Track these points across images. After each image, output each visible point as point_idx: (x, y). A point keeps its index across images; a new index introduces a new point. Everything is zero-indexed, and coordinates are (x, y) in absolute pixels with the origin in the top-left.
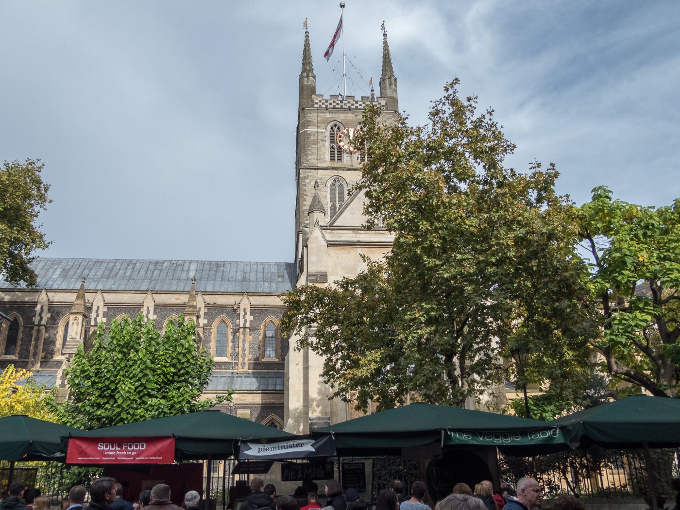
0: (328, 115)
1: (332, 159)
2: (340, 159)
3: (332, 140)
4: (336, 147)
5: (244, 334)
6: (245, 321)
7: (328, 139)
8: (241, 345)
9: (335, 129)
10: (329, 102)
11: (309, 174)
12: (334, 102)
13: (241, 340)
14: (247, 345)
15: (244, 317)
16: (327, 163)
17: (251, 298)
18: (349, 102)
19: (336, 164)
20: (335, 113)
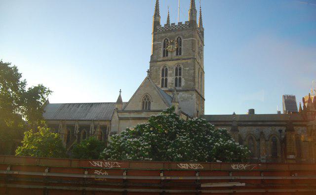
0: (163, 35)
1: (164, 56)
2: (167, 55)
3: (164, 47)
9: (166, 41)
16: (162, 59)
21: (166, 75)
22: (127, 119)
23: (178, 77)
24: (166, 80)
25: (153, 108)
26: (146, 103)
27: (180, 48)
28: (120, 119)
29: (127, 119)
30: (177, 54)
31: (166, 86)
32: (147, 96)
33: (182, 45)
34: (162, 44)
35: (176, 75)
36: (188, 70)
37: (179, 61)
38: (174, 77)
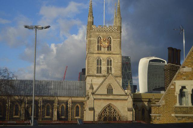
1: (98, 50)
2: (101, 50)
7: (97, 42)
9: (99, 38)
16: (97, 52)
20: (100, 32)
21: (101, 65)
22: (100, 99)
24: (101, 68)
25: (114, 93)
28: (94, 99)
29: (100, 99)
30: (108, 50)
31: (101, 72)
32: (110, 85)
35: (108, 65)
36: (117, 63)
37: (110, 55)
38: (106, 66)
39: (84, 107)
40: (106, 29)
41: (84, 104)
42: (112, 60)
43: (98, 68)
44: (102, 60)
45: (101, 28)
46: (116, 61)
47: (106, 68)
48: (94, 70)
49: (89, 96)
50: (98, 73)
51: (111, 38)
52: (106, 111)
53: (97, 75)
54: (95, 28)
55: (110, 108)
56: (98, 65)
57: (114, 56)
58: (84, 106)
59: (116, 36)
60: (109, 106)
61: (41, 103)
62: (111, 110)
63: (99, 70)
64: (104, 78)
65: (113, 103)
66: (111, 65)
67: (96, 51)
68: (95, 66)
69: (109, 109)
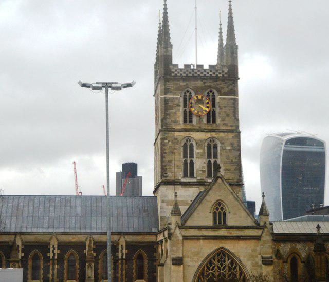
0: (182, 83)
1: (185, 121)
2: (191, 121)
3: (185, 105)
4: (188, 111)
5: (122, 264)
6: (123, 254)
7: (182, 104)
8: (120, 271)
10: (185, 71)
11: (169, 135)
12: (187, 71)
13: (120, 269)
14: (124, 272)
15: (122, 251)
16: (182, 126)
17: (126, 237)
18: (199, 71)
19: (188, 126)
20: (188, 81)
21: (192, 156)
23: (212, 160)
24: (192, 163)
25: (231, 221)
26: (220, 213)
27: (214, 113)
28: (185, 238)
30: (208, 121)
31: (192, 175)
32: (220, 204)
33: (217, 106)
34: (182, 100)
35: (209, 156)
36: (230, 150)
37: (214, 134)
38: (206, 161)
39: (155, 257)
40: (202, 73)
41: (155, 251)
42: (219, 145)
43: (186, 163)
44: (195, 144)
45: (191, 71)
46: (229, 148)
47: (206, 165)
48: (176, 169)
49: (172, 231)
50: (185, 175)
51: (213, 93)
52: (213, 265)
53: (185, 181)
54: (176, 71)
55: (221, 258)
56: (185, 156)
57: (222, 135)
58: (155, 254)
59: (225, 90)
60: (221, 254)
61: (54, 249)
62: (224, 261)
63: (189, 169)
64: (202, 189)
65: (229, 246)
66: (216, 156)
67: (180, 124)
68: (179, 158)
69: (218, 261)
